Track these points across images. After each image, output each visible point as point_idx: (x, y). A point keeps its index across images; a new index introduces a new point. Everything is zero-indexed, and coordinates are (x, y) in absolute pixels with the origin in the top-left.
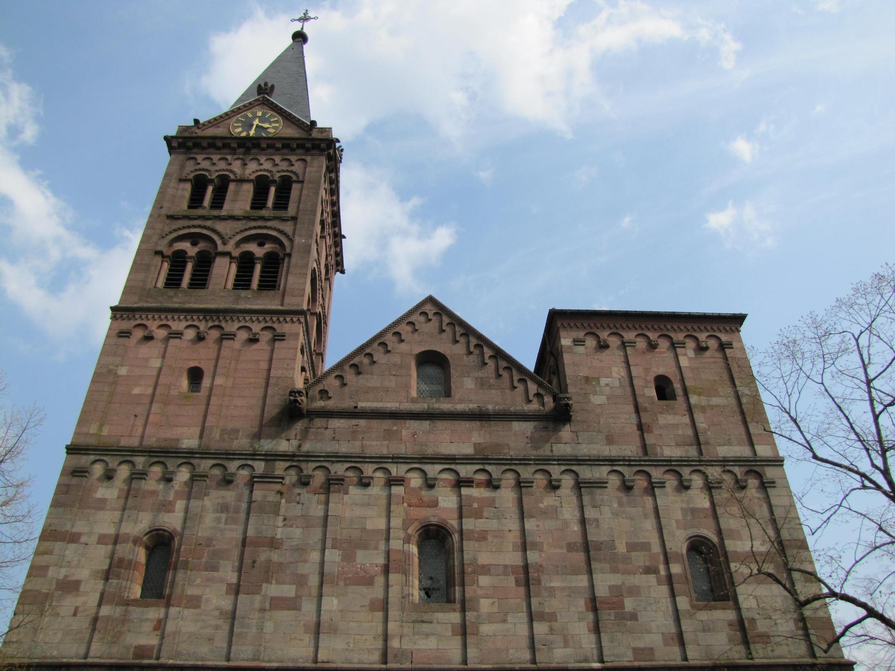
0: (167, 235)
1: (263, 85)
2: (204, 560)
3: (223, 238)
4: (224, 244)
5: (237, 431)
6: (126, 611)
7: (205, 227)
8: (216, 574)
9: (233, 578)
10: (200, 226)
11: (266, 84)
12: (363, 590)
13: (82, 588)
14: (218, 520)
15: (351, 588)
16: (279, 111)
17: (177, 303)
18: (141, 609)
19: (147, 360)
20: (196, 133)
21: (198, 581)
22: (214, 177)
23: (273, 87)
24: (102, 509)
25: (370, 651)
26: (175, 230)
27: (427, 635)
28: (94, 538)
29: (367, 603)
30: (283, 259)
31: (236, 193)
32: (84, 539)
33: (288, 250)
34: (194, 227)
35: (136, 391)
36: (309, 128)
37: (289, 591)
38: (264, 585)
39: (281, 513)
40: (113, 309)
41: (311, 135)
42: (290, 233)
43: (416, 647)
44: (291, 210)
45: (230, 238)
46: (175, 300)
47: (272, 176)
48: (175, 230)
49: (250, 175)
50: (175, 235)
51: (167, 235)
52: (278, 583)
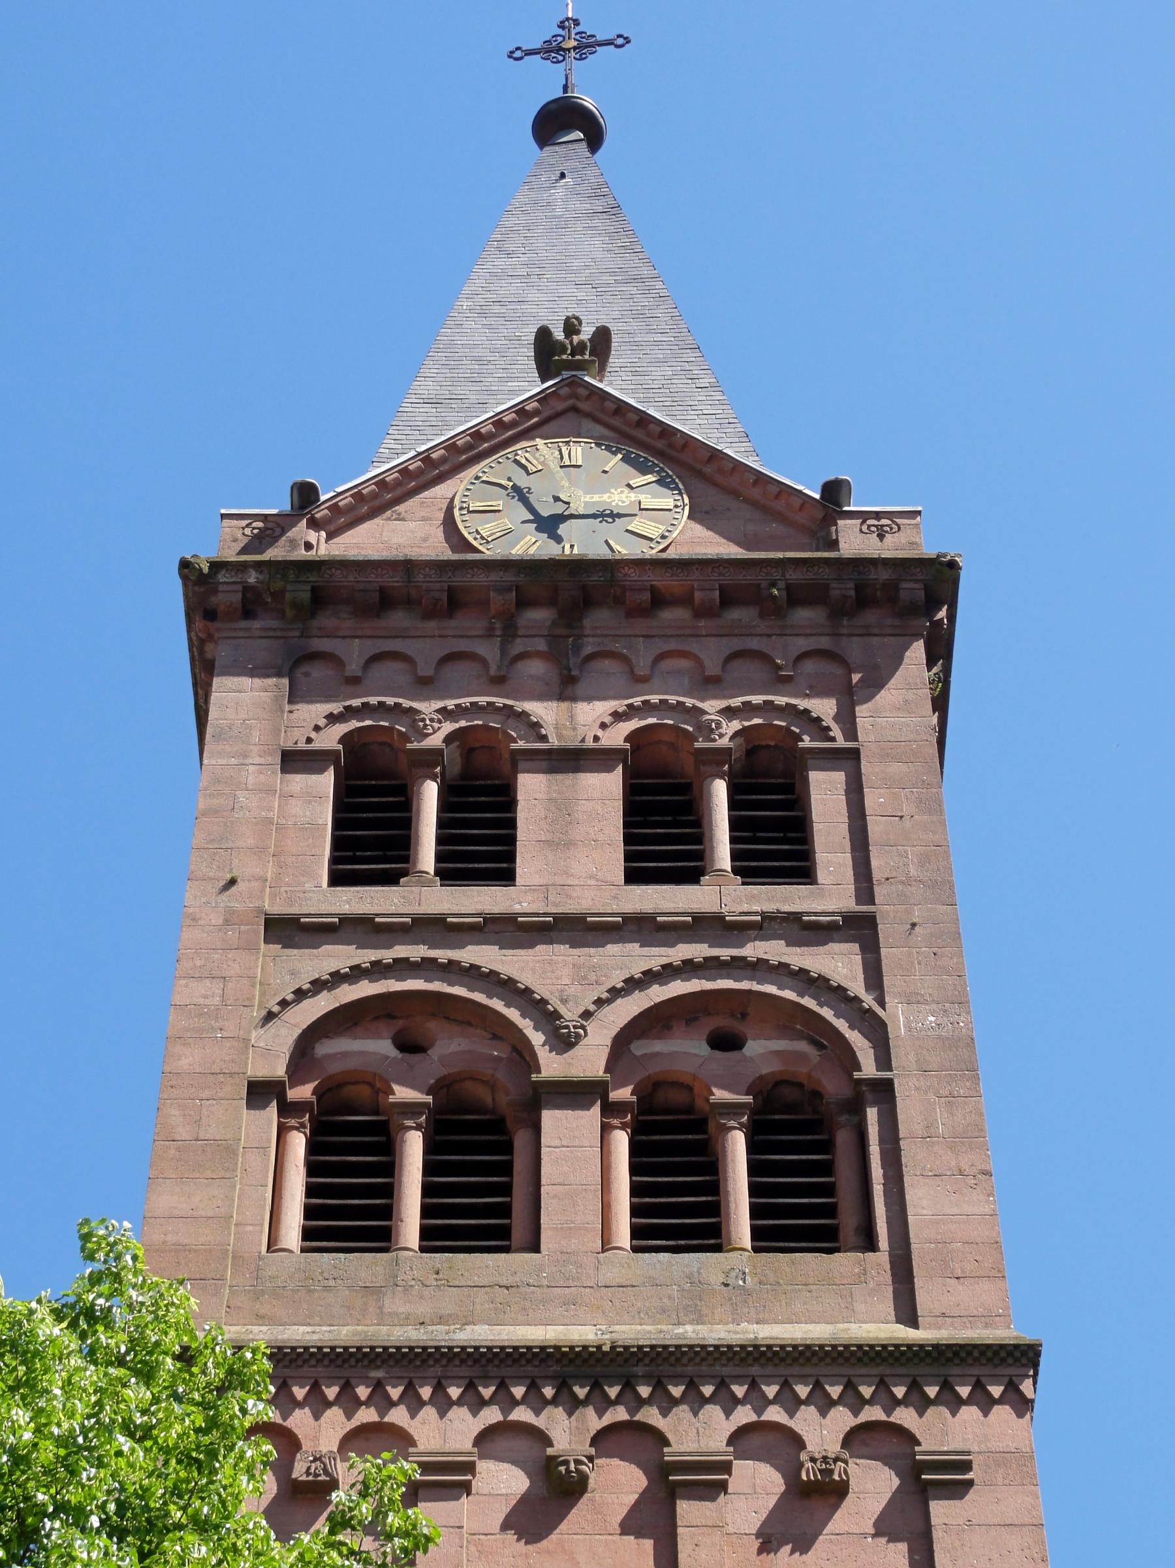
0: (284, 1004)
1: (559, 334)
3: (555, 1015)
4: (564, 1042)
7: (452, 970)
10: (427, 967)
11: (571, 327)
16: (660, 444)
17: (407, 1320)
20: (308, 546)
22: (435, 740)
23: (603, 337)
26: (319, 986)
30: (856, 1108)
31: (562, 810)
33: (869, 1068)
34: (402, 967)
36: (819, 515)
41: (834, 545)
42: (857, 986)
45: (587, 1015)
46: (395, 1304)
47: (707, 730)
48: (319, 986)
49: (603, 726)
50: (323, 1004)
51: (284, 1004)
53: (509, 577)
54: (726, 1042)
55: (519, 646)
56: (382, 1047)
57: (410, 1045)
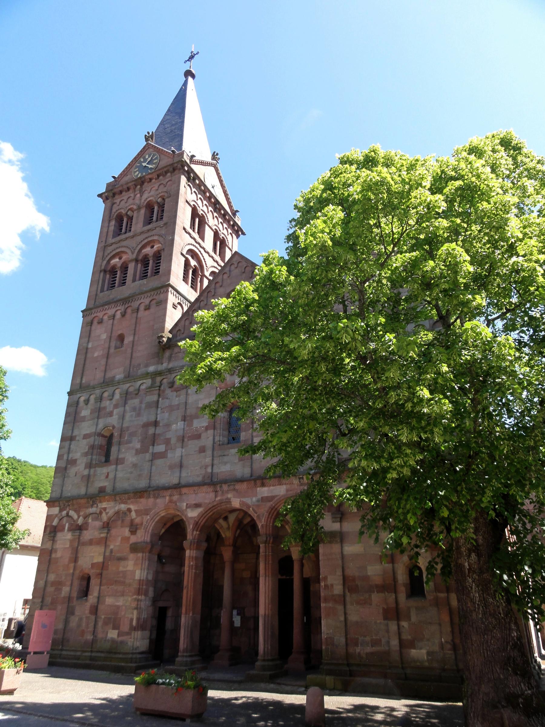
2: (126, 438)
5: (139, 365)
6: (95, 471)
8: (131, 445)
9: (138, 446)
12: (196, 441)
13: (78, 462)
14: (132, 416)
15: (190, 442)
18: (100, 468)
19: (99, 336)
21: (123, 450)
24: (84, 421)
25: (198, 476)
27: (226, 463)
28: (82, 436)
29: (197, 449)
32: (77, 438)
35: (96, 355)
37: (160, 448)
38: (151, 447)
39: (159, 406)
40: (82, 311)
43: (220, 471)
44: (165, 219)
52: (158, 445)
53: (134, 183)
54: (152, 247)
55: (136, 193)
56: (117, 260)
57: (120, 258)
